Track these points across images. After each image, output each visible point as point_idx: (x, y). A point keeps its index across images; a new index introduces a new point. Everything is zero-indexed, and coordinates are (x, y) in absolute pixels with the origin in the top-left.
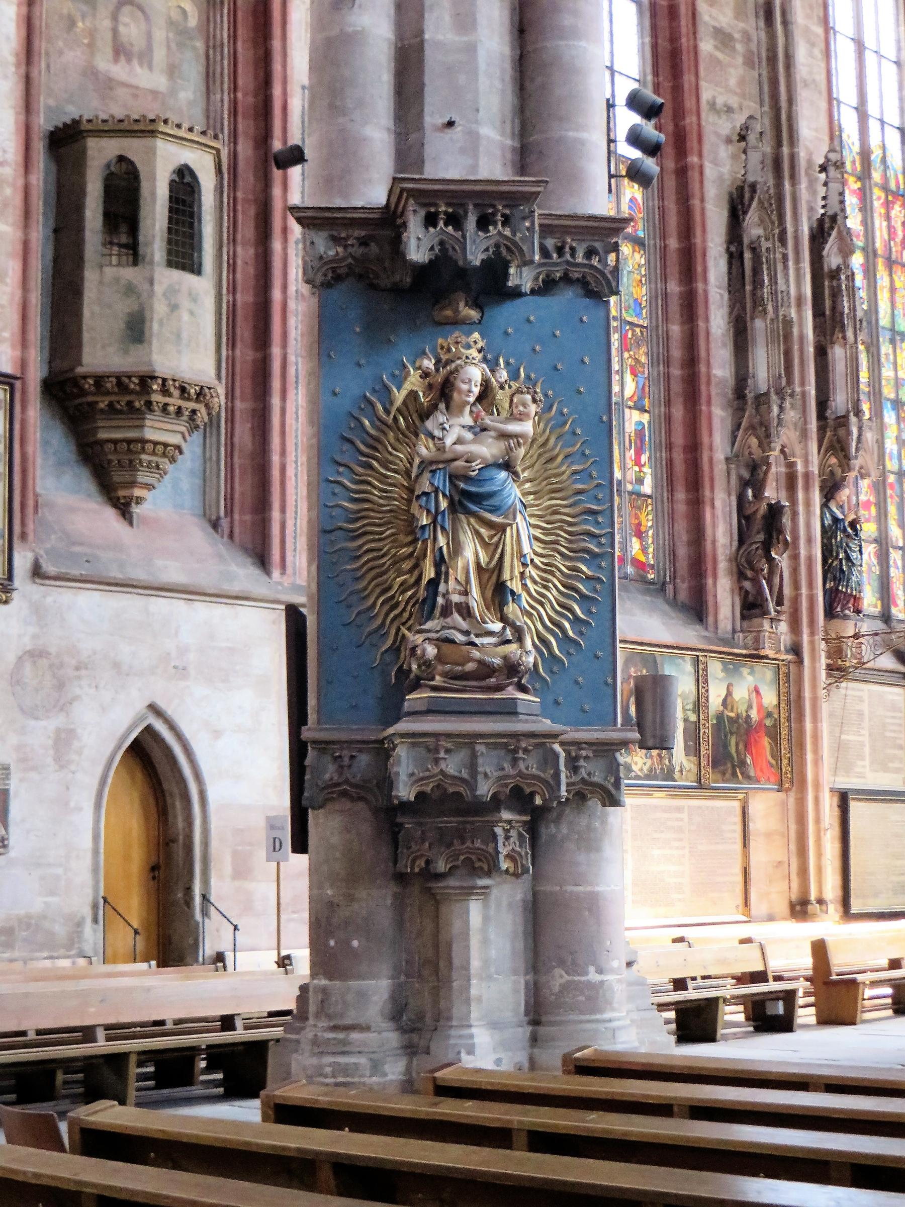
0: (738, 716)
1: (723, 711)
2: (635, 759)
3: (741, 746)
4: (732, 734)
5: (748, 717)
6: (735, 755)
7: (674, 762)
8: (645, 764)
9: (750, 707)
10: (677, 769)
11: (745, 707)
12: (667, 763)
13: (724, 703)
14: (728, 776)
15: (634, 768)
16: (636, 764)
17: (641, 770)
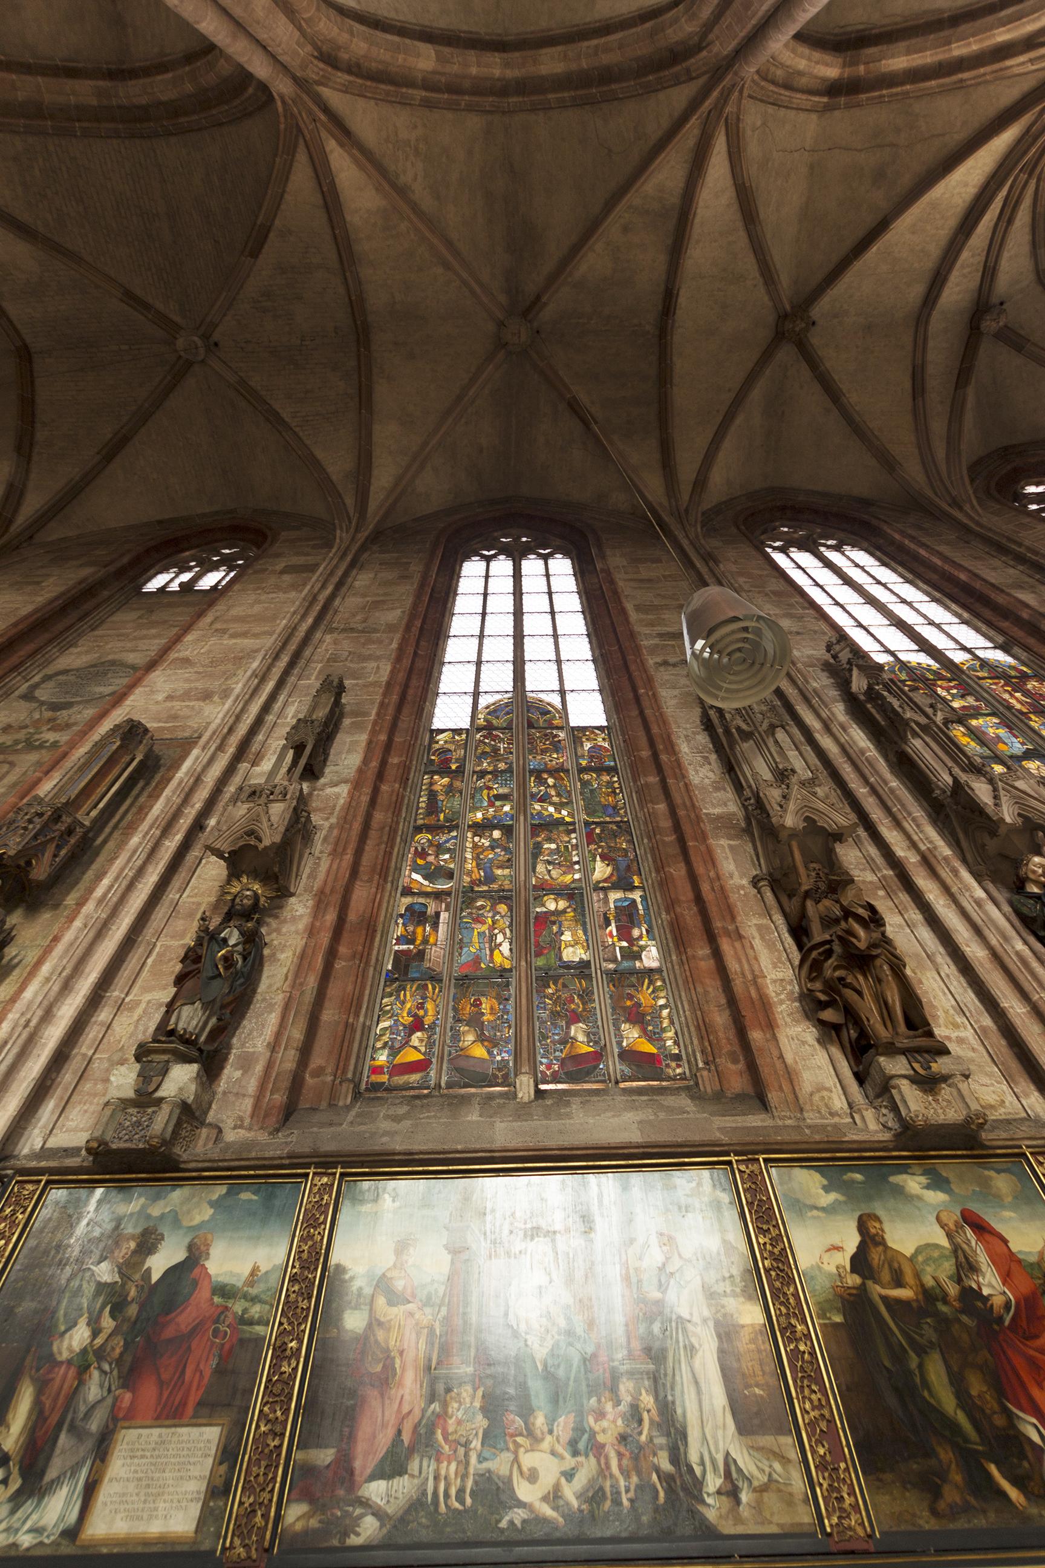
0: (931, 1296)
1: (863, 1288)
2: (528, 1460)
3: (976, 1386)
4: (921, 1351)
5: (971, 1297)
6: (962, 1418)
7: (693, 1457)
8: (569, 1475)
9: (966, 1266)
10: (713, 1482)
11: (948, 1267)
12: (666, 1466)
13: (860, 1263)
14: (951, 1495)
15: (524, 1491)
16: (532, 1477)
17: (554, 1497)
